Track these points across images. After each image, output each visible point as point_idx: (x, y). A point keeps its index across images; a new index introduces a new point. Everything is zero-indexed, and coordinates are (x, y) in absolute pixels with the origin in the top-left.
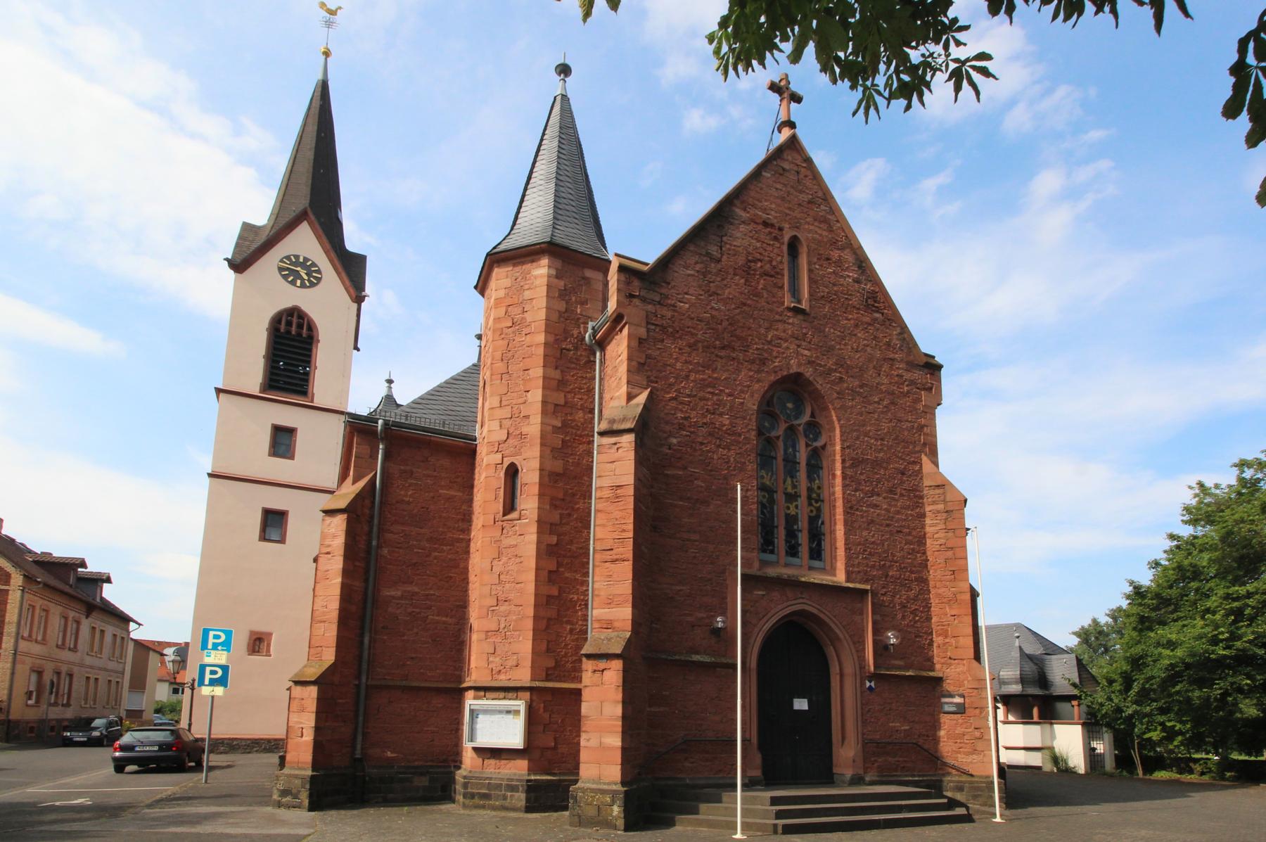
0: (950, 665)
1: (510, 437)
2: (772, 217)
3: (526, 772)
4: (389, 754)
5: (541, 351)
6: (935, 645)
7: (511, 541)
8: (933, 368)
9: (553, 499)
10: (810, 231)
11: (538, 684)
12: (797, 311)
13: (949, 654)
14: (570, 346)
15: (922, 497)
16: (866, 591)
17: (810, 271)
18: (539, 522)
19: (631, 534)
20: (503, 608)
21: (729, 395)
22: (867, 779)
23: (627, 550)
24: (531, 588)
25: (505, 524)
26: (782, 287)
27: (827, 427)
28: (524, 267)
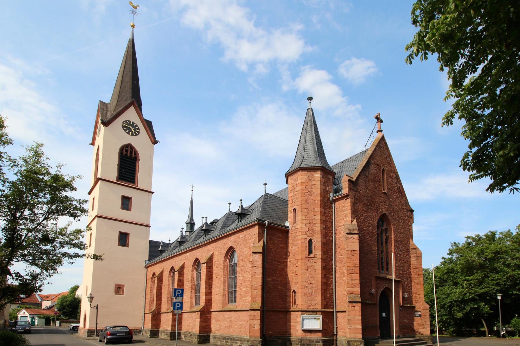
0: (418, 303)
1: (310, 230)
2: (378, 162)
3: (321, 337)
4: (271, 333)
5: (319, 202)
6: (413, 297)
7: (312, 264)
8: (412, 211)
9: (324, 251)
10: (386, 167)
11: (323, 310)
12: (385, 193)
13: (417, 299)
14: (326, 201)
15: (410, 252)
16: (400, 281)
17: (387, 180)
18: (321, 259)
19: (359, 266)
20: (310, 286)
21: (371, 220)
22: (401, 336)
23: (358, 270)
24: (320, 280)
25: (309, 259)
26: (381, 186)
27: (389, 230)
28: (311, 173)
